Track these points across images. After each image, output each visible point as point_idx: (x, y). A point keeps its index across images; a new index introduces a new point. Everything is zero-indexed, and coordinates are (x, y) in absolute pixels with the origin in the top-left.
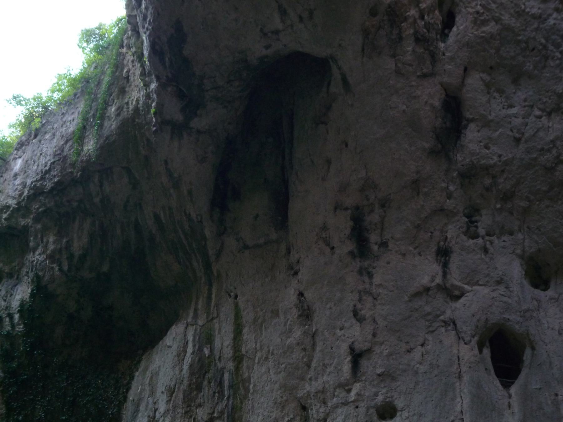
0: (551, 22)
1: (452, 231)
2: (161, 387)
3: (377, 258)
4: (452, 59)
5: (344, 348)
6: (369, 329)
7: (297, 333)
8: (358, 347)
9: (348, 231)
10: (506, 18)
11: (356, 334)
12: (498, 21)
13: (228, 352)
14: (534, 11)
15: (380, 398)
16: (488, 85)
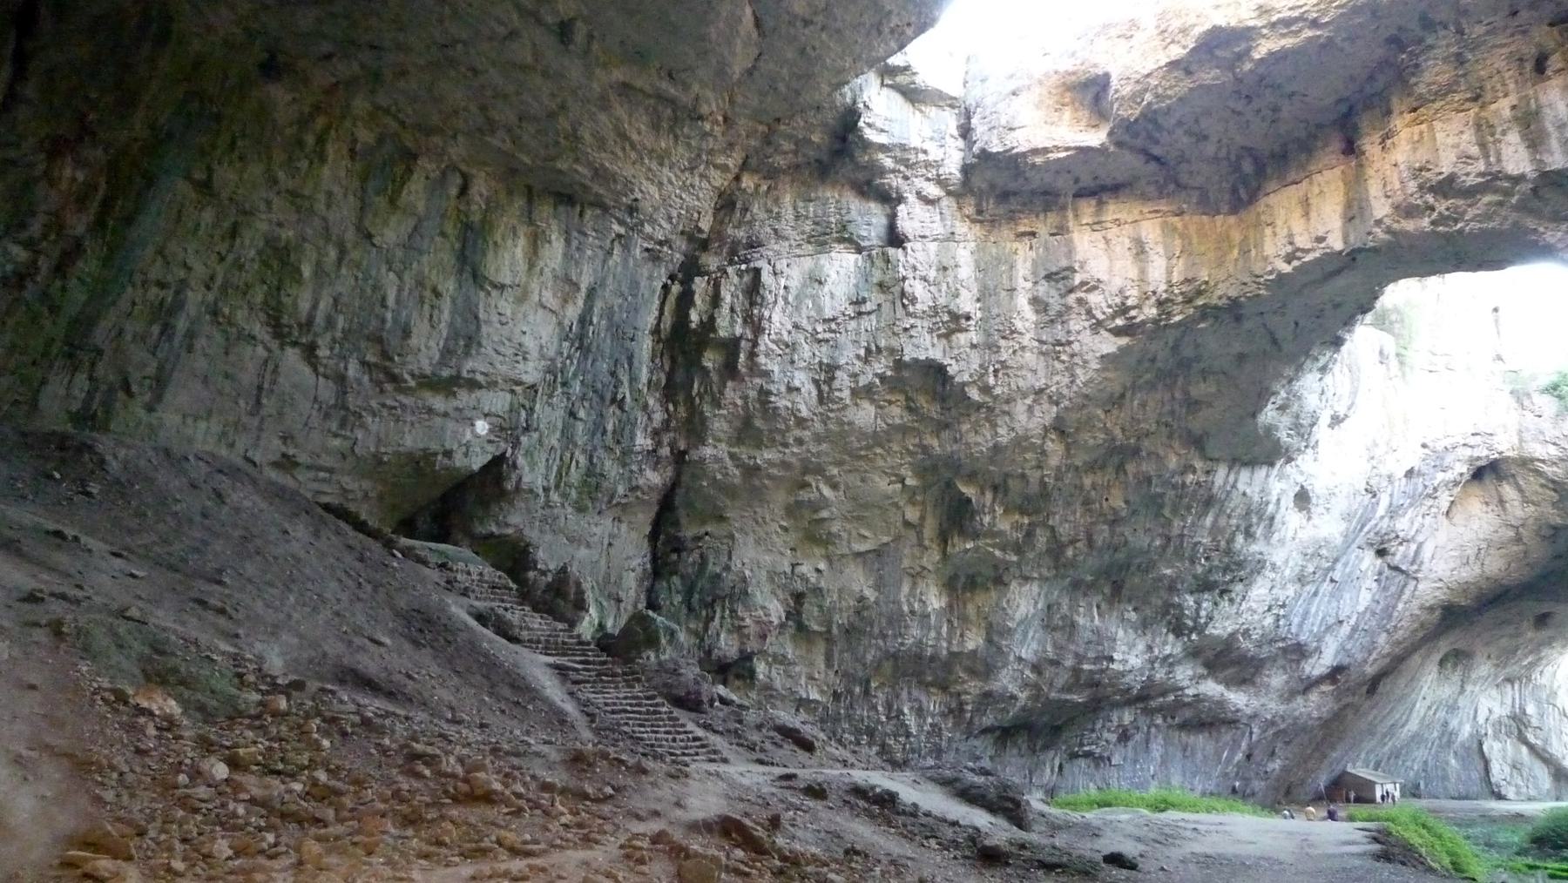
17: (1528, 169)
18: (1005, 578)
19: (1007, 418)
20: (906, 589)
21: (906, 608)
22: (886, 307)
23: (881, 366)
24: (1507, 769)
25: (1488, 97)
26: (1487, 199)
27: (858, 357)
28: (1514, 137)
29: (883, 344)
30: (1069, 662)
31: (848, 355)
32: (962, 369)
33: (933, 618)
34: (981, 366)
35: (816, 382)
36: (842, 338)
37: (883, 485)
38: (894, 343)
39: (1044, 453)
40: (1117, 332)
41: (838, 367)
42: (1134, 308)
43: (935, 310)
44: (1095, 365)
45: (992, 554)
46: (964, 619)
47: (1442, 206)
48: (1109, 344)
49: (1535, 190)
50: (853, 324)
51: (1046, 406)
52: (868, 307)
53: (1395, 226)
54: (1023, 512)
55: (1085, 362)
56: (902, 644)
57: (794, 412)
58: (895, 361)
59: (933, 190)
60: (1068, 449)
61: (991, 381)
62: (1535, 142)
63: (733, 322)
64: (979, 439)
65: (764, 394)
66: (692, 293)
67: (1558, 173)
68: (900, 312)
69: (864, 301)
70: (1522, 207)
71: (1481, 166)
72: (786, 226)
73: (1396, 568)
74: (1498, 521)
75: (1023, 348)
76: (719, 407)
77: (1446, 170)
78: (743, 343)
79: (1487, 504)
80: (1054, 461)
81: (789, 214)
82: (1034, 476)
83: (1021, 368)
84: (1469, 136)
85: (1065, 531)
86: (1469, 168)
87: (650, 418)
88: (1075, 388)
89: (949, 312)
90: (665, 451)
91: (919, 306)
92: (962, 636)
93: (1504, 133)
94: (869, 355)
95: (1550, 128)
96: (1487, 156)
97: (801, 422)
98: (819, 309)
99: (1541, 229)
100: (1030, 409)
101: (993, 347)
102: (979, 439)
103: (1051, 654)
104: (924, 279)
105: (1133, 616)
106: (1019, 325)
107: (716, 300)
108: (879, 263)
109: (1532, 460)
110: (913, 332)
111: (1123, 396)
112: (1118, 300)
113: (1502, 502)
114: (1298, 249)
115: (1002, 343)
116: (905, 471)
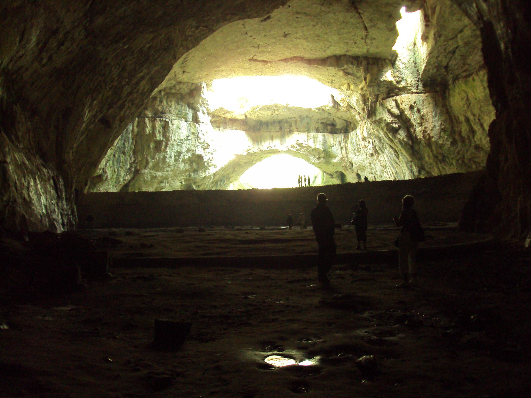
22: (193, 138)
28: (312, 140)
31: (184, 150)
35: (175, 156)
36: (183, 145)
47: (298, 148)
50: (185, 142)
52: (190, 138)
57: (169, 163)
59: (205, 111)
63: (160, 136)
65: (165, 157)
66: (145, 123)
68: (197, 142)
71: (306, 143)
72: (172, 109)
76: (153, 159)
78: (164, 143)
81: (173, 107)
82: (207, 183)
87: (131, 159)
90: (133, 169)
94: (188, 151)
97: (169, 166)
98: (179, 135)
107: (154, 128)
108: (193, 127)
116: (183, 180)
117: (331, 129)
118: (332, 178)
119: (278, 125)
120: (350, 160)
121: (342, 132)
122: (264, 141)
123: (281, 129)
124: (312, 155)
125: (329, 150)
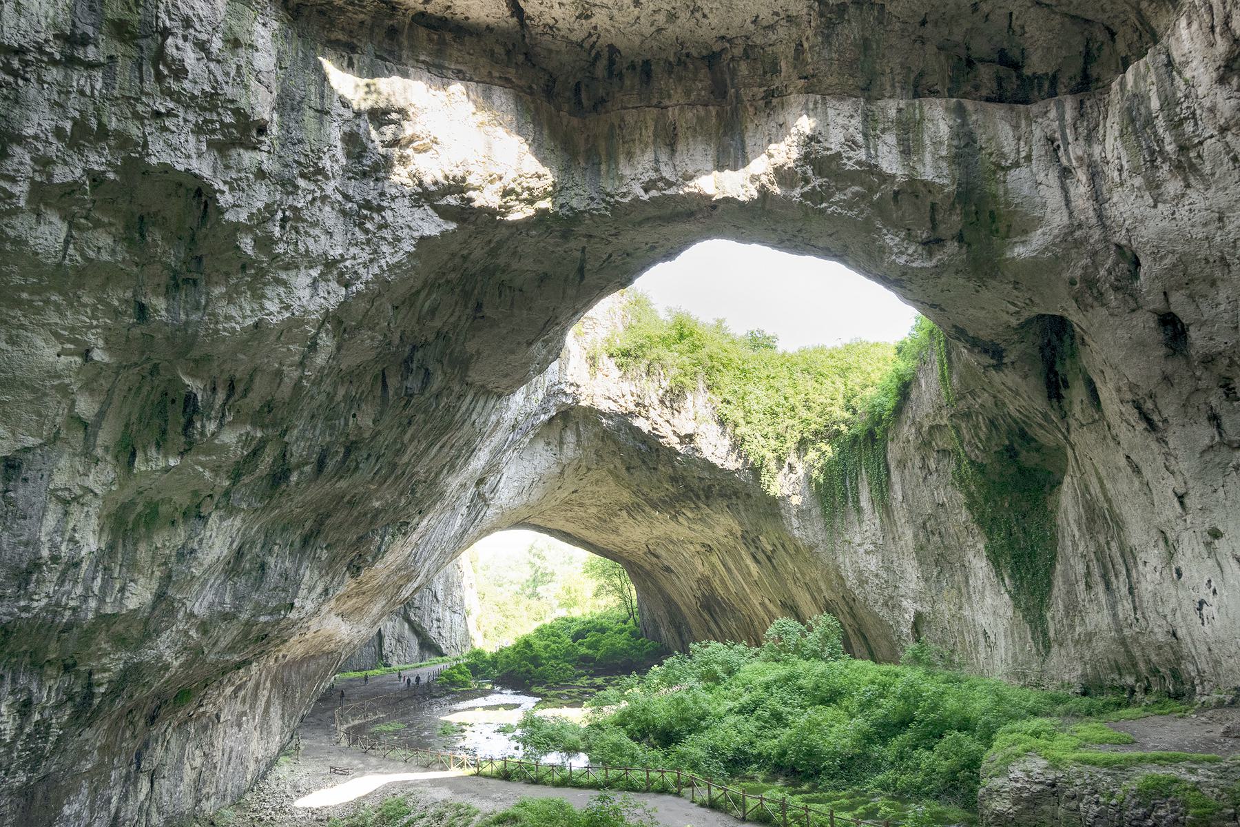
0: (1218, 239)
1: (1214, 401)
2: (1072, 522)
3: (1165, 430)
4: (1149, 292)
5: (1170, 493)
6: (1180, 479)
7: (1137, 483)
8: (1180, 491)
9: (1137, 415)
10: (1179, 248)
11: (1173, 483)
12: (1173, 252)
13: (1101, 498)
14: (1200, 236)
15: (1207, 525)
16: (1191, 297)
17: (899, 173)
18: (204, 511)
19: (281, 290)
20: (50, 521)
21: (45, 553)
23: (96, 161)
24: (393, 642)
25: (875, 93)
26: (856, 188)
27: (59, 132)
28: (891, 138)
29: (113, 124)
30: (244, 616)
32: (239, 206)
33: (84, 566)
34: (267, 206)
36: (32, 91)
37: (48, 353)
38: (134, 130)
39: (313, 347)
40: (445, 213)
41: (20, 140)
42: (474, 189)
43: (212, 100)
44: (408, 246)
45: (200, 476)
46: (132, 565)
47: (816, 182)
48: (432, 226)
49: (896, 194)
50: (54, 74)
51: (334, 285)
52: (91, 53)
53: (769, 185)
54: (257, 419)
55: (398, 239)
56: (26, 609)
58: (128, 160)
60: (339, 348)
61: (277, 231)
62: (908, 150)
64: (233, 311)
67: (925, 184)
69: (85, 41)
70: (879, 207)
71: (862, 155)
73: (480, 496)
74: (552, 459)
75: (324, 198)
77: (835, 148)
79: (549, 444)
80: (320, 359)
83: (315, 225)
84: (857, 122)
85: (298, 450)
86: (852, 154)
88: (376, 270)
89: (237, 112)
91: (187, 84)
92: (122, 590)
93: (884, 131)
94: (82, 136)
95: (928, 142)
96: (868, 148)
99: (885, 231)
100: (314, 284)
101: (288, 186)
102: (233, 311)
103: (228, 608)
104: (202, 46)
105: (325, 555)
106: (326, 162)
109: (599, 412)
110: (169, 123)
111: (418, 292)
112: (459, 173)
113: (561, 443)
114: (662, 179)
115: (301, 182)
116: (93, 338)
117: (1000, 80)
118: (998, 367)
119: (704, 72)
120: (1120, 238)
121: (1061, 88)
122: (630, 155)
123: (719, 91)
124: (896, 226)
125: (992, 188)
